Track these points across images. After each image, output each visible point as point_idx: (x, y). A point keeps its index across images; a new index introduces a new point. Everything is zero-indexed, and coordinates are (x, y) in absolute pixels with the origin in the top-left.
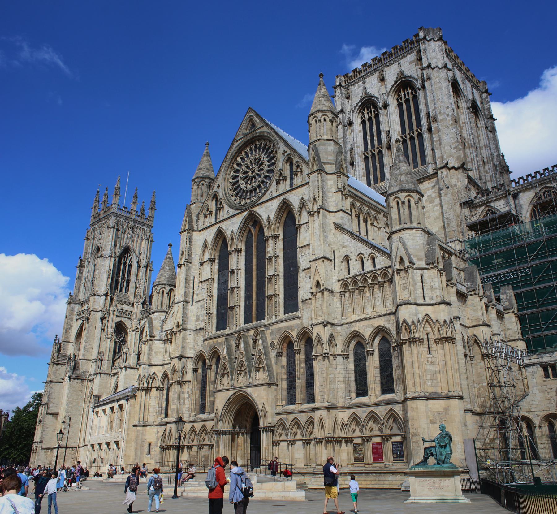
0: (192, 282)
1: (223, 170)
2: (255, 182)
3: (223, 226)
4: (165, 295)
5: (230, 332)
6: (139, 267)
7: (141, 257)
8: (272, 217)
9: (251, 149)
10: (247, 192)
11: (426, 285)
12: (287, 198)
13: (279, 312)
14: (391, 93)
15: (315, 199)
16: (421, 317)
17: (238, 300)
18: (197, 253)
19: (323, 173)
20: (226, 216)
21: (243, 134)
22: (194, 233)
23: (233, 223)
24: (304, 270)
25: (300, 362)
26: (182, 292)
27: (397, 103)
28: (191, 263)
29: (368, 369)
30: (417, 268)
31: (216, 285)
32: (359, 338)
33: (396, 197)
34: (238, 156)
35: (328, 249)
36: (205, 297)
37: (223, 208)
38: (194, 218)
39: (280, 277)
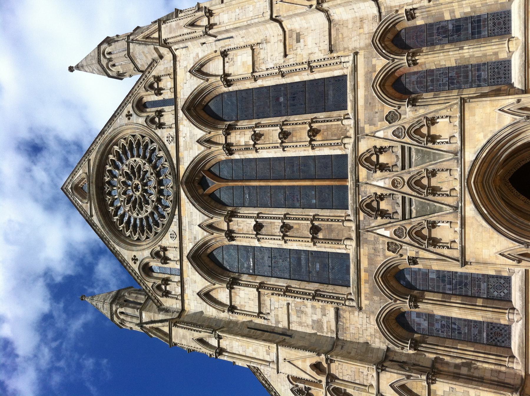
0: (253, 330)
1: (117, 248)
3: (188, 247)
8: (199, 133)
10: (159, 200)
12: (183, 103)
20: (177, 242)
21: (87, 203)
23: (190, 223)
24: (286, 55)
28: (223, 327)
31: (272, 281)
36: (283, 301)
37: (165, 249)
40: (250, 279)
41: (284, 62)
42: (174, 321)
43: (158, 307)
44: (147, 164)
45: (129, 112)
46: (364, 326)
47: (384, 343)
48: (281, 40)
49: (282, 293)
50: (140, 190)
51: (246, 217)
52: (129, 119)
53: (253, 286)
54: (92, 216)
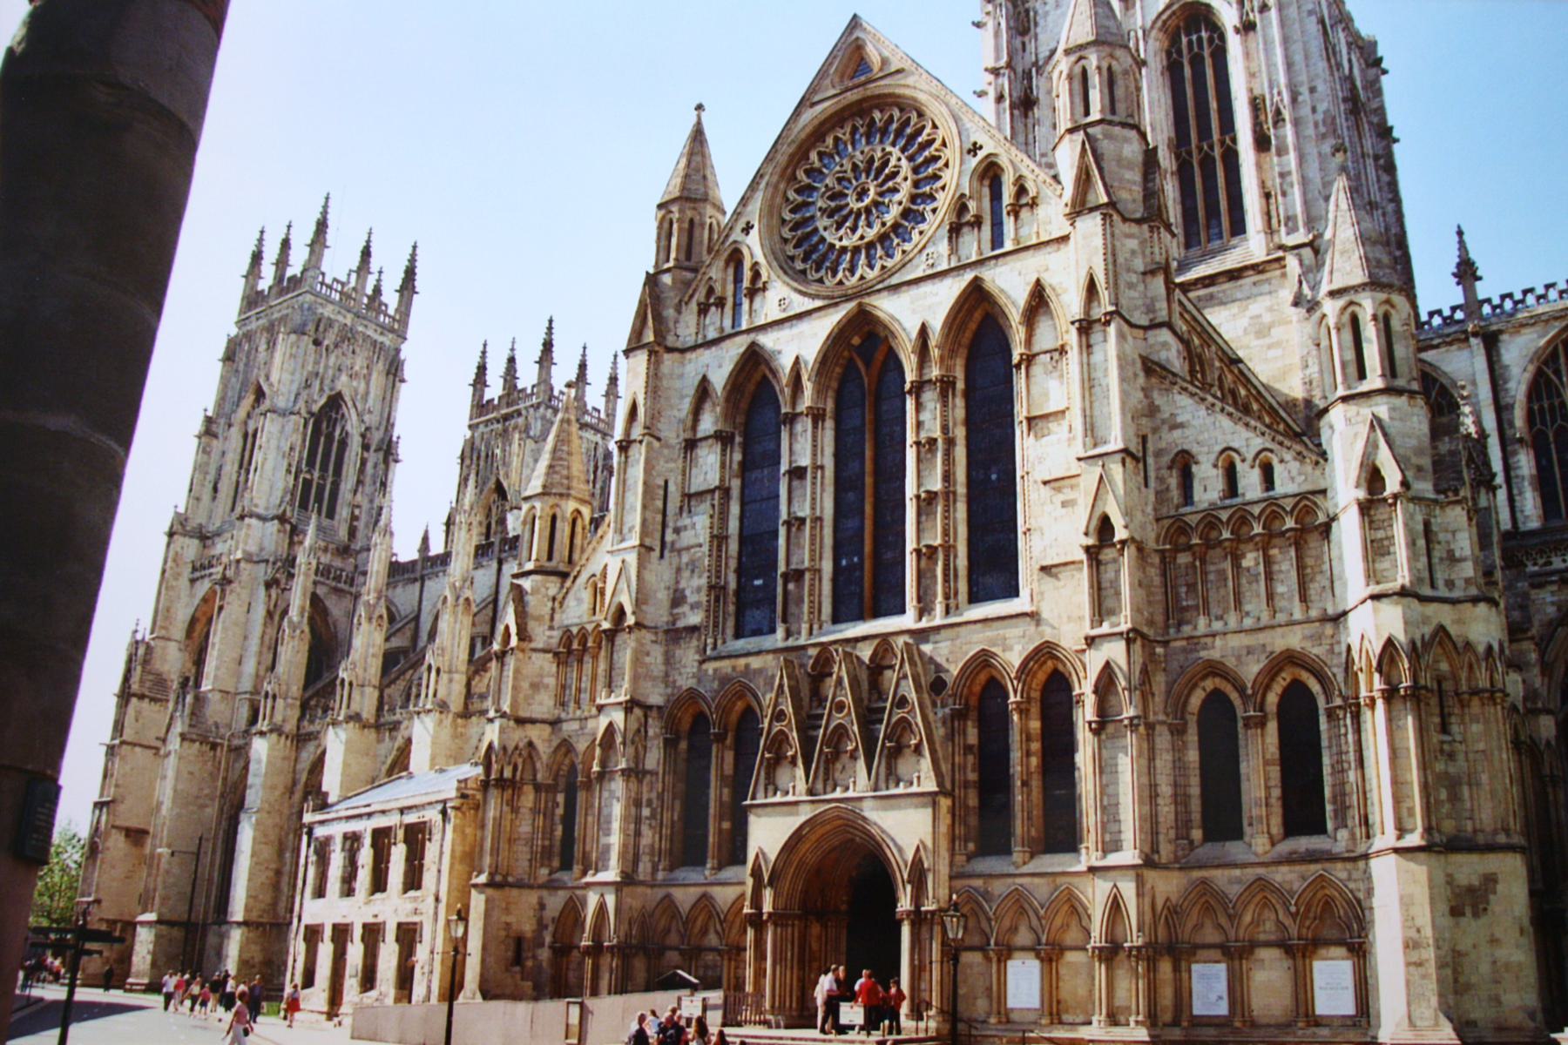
0: (661, 492)
2: (870, 225)
3: (768, 340)
5: (791, 642)
6: (366, 447)
8: (937, 324)
9: (854, 130)
10: (844, 250)
11: (1437, 547)
13: (956, 594)
14: (1154, 33)
15: (1091, 288)
16: (1427, 630)
17: (816, 555)
18: (676, 413)
19: (1116, 217)
22: (666, 356)
24: (1045, 483)
25: (1029, 739)
26: (635, 519)
27: (1165, 63)
28: (659, 439)
29: (1243, 768)
30: (1413, 500)
31: (735, 509)
32: (1217, 680)
33: (1351, 303)
34: (813, 146)
35: (1131, 431)
38: (670, 313)
39: (959, 498)
40: (735, 466)
41: (1035, 482)
42: (657, 348)
43: (680, 301)
44: (901, 208)
45: (981, 148)
46: (683, 670)
47: (668, 701)
48: (1069, 469)
49: (715, 532)
50: (861, 205)
51: (815, 446)
52: (969, 152)
53: (722, 480)
54: (813, 105)
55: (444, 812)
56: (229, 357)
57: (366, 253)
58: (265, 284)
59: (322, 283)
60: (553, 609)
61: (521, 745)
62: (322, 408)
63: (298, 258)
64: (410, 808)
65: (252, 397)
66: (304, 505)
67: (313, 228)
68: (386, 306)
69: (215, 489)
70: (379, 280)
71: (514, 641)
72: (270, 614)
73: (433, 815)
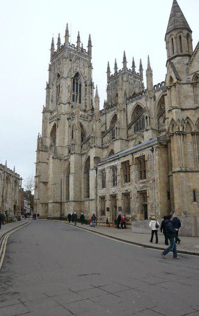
4: (183, 38)
6: (86, 86)
7: (87, 79)
55: (152, 151)
56: (50, 70)
57: (79, 37)
58: (55, 50)
59: (70, 46)
60: (188, 69)
61: (184, 119)
62: (75, 76)
63: (63, 42)
64: (136, 152)
65: (57, 77)
66: (73, 101)
67: (65, 32)
68: (85, 50)
69: (52, 101)
70: (82, 46)
71: (175, 81)
72: (69, 126)
73: (147, 153)
